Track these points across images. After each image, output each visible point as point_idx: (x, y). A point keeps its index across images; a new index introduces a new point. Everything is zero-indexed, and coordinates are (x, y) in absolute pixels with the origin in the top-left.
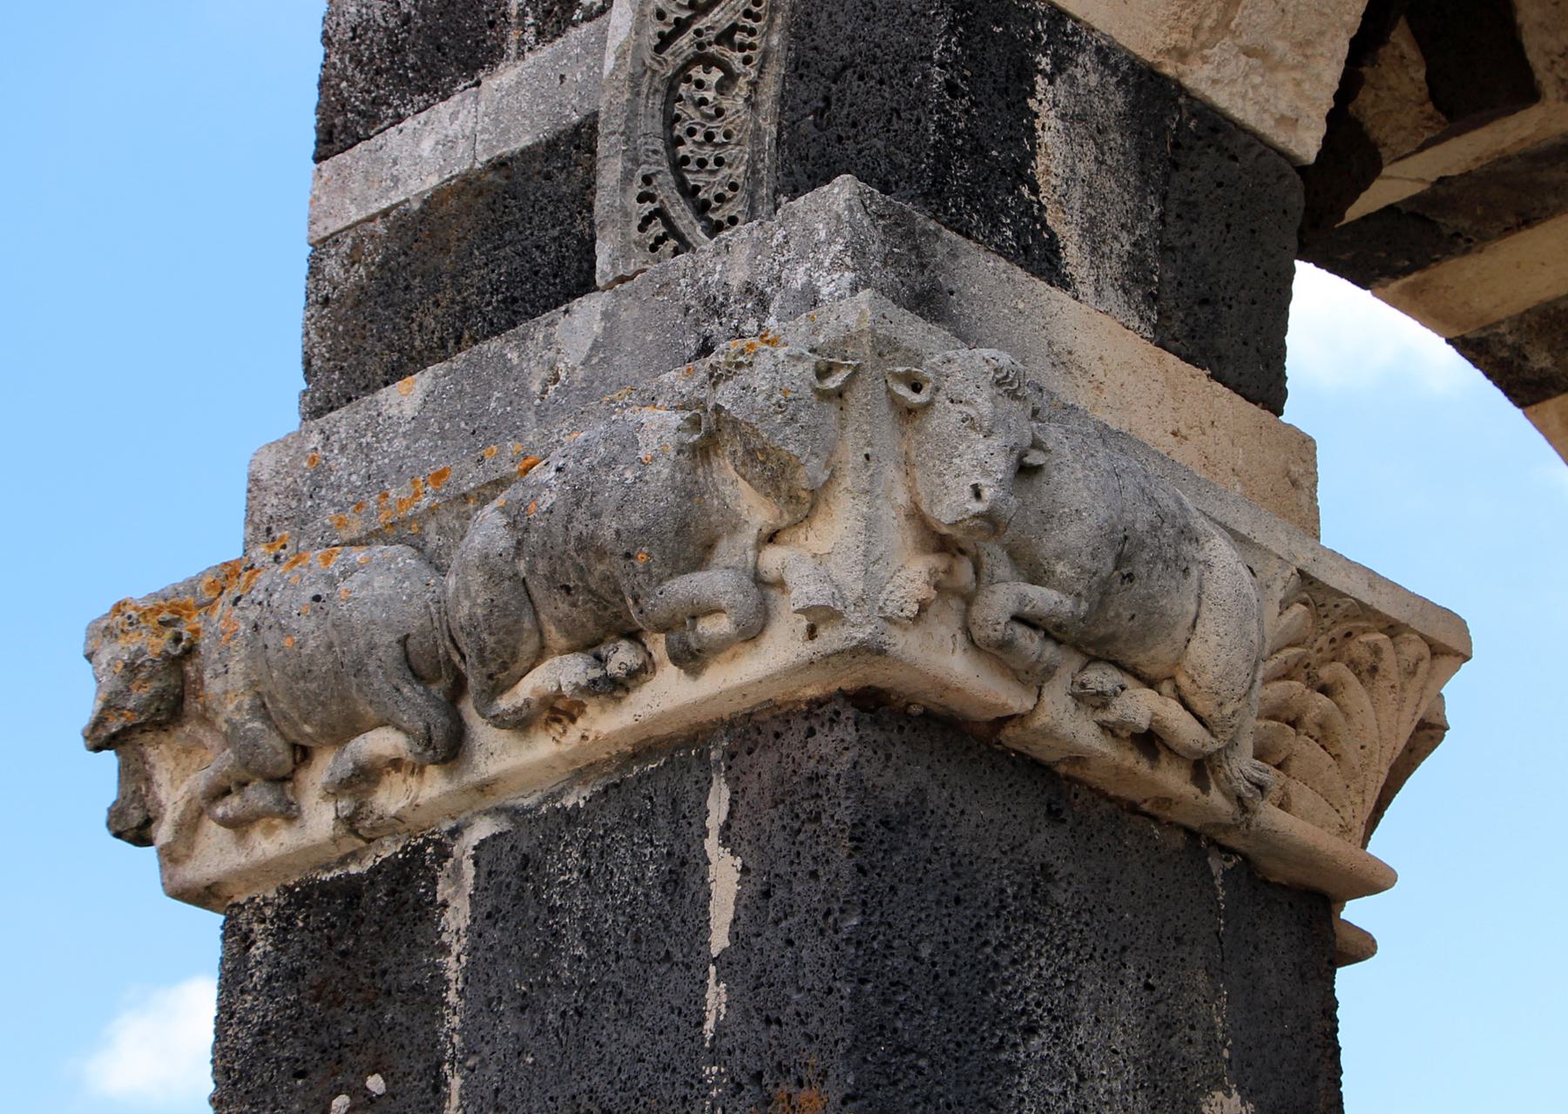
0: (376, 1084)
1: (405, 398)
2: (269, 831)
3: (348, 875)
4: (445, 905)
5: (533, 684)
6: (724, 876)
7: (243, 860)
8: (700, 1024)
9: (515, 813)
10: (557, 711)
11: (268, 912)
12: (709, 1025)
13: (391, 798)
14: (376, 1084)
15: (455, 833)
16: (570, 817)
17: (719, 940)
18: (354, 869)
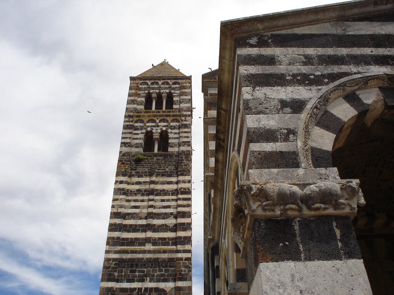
0: (287, 243)
1: (275, 170)
2: (269, 212)
3: (277, 219)
4: (294, 226)
5: (317, 205)
6: (338, 232)
7: (265, 214)
8: (338, 246)
9: (303, 218)
10: (318, 209)
11: (263, 220)
12: (339, 246)
13: (290, 213)
14: (287, 243)
15: (294, 218)
16: (312, 221)
17: (339, 238)
18: (277, 219)
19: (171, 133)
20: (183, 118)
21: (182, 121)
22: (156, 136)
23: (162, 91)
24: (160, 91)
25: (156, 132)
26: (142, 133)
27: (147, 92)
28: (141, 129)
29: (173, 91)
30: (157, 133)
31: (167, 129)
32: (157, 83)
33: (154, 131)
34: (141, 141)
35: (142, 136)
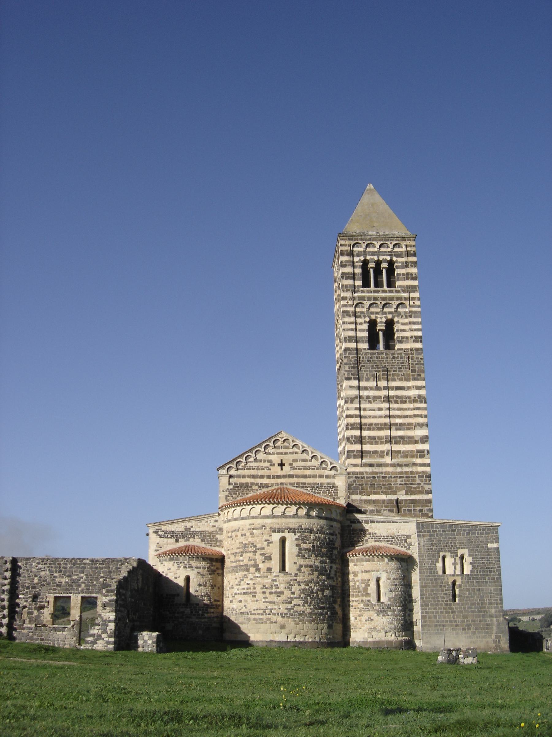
19: (398, 322)
20: (411, 303)
21: (410, 306)
22: (381, 327)
23: (381, 258)
24: (378, 257)
25: (381, 320)
26: (365, 322)
27: (362, 258)
28: (365, 317)
29: (394, 259)
30: (381, 322)
31: (393, 317)
32: (374, 246)
33: (379, 320)
34: (366, 334)
35: (366, 326)
